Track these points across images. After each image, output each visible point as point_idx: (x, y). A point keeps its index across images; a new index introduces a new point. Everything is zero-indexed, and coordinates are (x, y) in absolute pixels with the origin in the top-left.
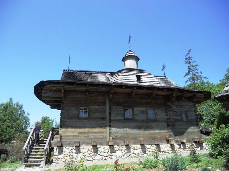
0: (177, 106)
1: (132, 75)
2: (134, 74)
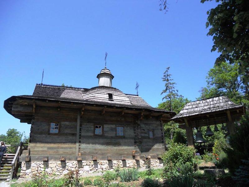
1: (104, 93)
2: (107, 92)
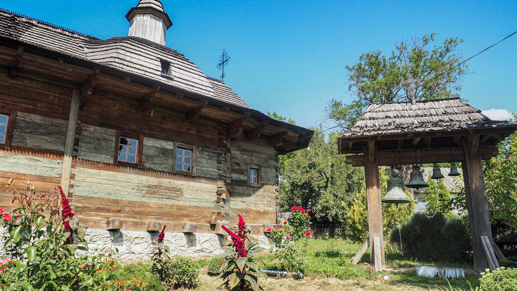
2: (159, 56)
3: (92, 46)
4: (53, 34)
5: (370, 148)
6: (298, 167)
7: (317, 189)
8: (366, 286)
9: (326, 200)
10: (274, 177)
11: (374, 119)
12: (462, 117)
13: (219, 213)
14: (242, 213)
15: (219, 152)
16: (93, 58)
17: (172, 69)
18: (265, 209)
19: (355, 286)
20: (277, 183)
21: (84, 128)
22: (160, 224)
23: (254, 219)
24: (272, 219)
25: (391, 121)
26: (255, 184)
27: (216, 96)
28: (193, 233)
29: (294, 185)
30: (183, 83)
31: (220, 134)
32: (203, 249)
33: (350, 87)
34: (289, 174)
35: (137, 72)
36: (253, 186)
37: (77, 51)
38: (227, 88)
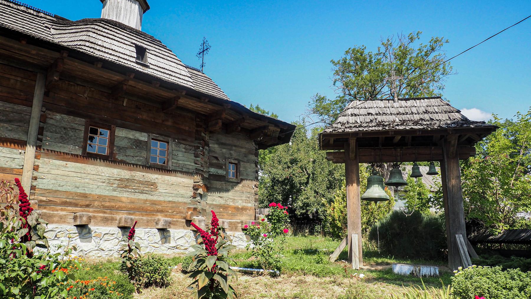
0: (222, 144)
1: (122, 41)
2: (134, 41)
3: (59, 27)
4: (15, 11)
5: (350, 145)
6: (280, 162)
7: (299, 185)
8: (342, 283)
9: (307, 196)
10: (254, 172)
11: (355, 115)
12: (443, 117)
13: (195, 209)
14: (220, 209)
15: (196, 145)
16: (60, 40)
17: (148, 56)
18: (244, 205)
19: (331, 283)
20: (256, 179)
21: (49, 116)
22: (131, 219)
23: (232, 216)
24: (250, 215)
25: (373, 118)
26: (234, 180)
27: (195, 86)
28: (168, 229)
29: (274, 181)
30: (160, 71)
31: (198, 126)
32: (177, 245)
33: (335, 82)
34: (270, 169)
35: (109, 58)
36: (231, 181)
37: (43, 32)
38: (207, 78)
